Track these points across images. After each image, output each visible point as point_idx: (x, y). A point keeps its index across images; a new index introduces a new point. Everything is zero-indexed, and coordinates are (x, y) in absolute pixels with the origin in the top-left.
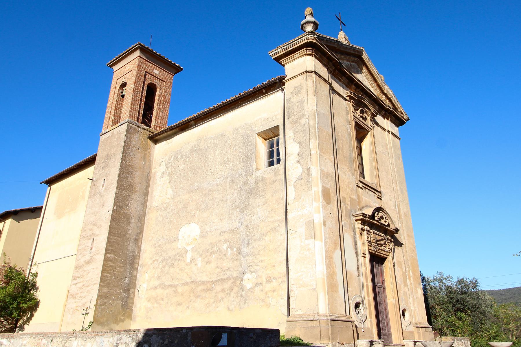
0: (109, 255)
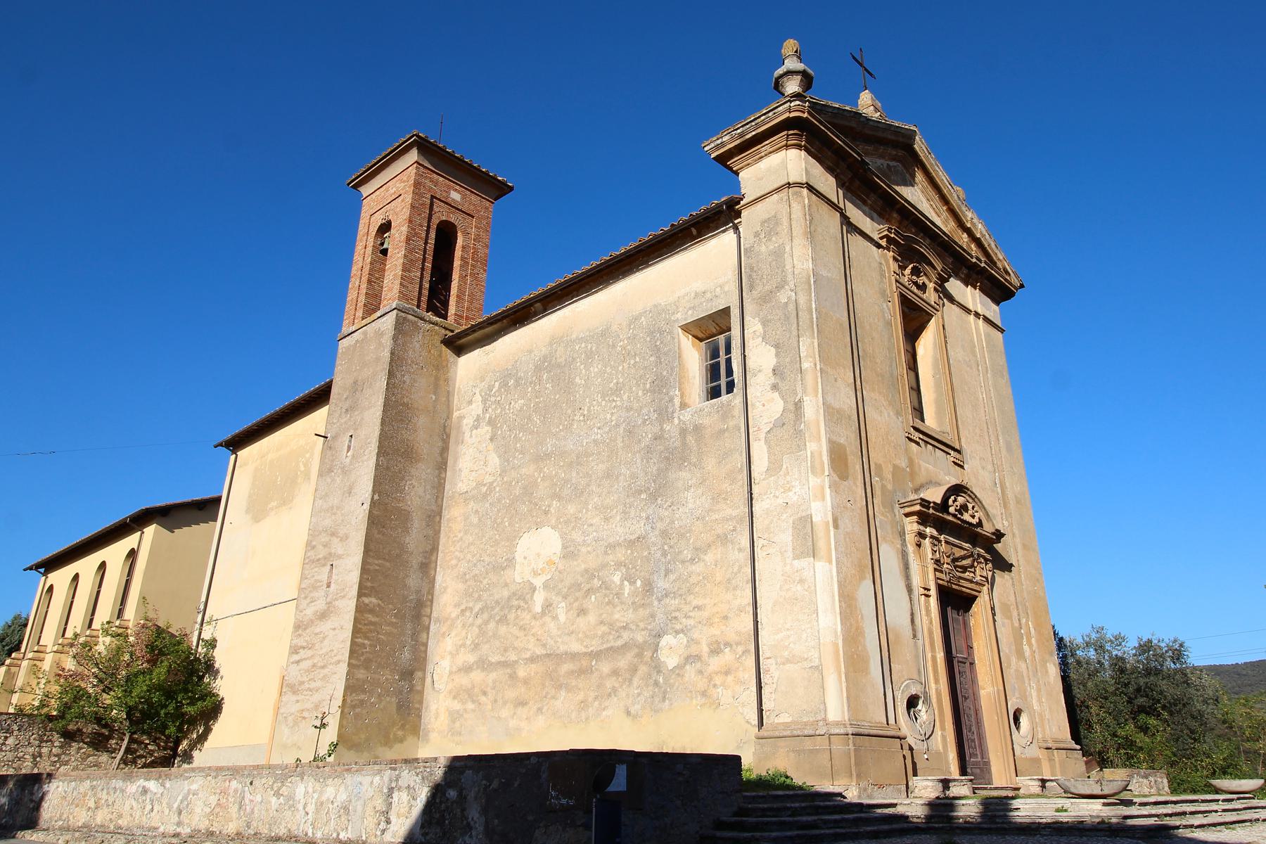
0: (366, 600)
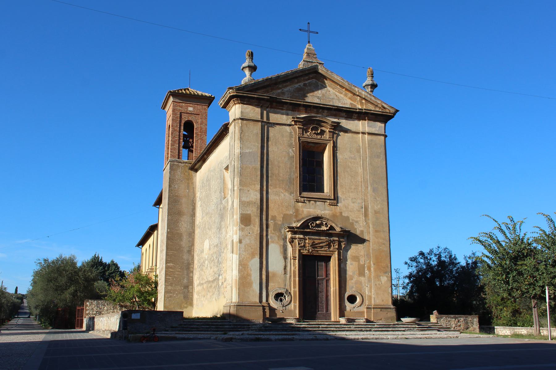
0: (169, 264)
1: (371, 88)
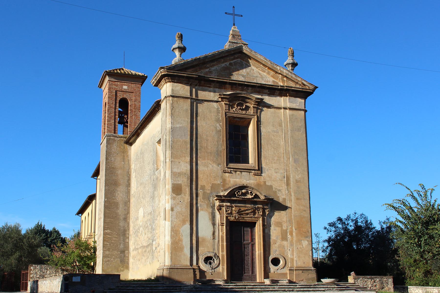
0: (106, 231)
1: (292, 66)
